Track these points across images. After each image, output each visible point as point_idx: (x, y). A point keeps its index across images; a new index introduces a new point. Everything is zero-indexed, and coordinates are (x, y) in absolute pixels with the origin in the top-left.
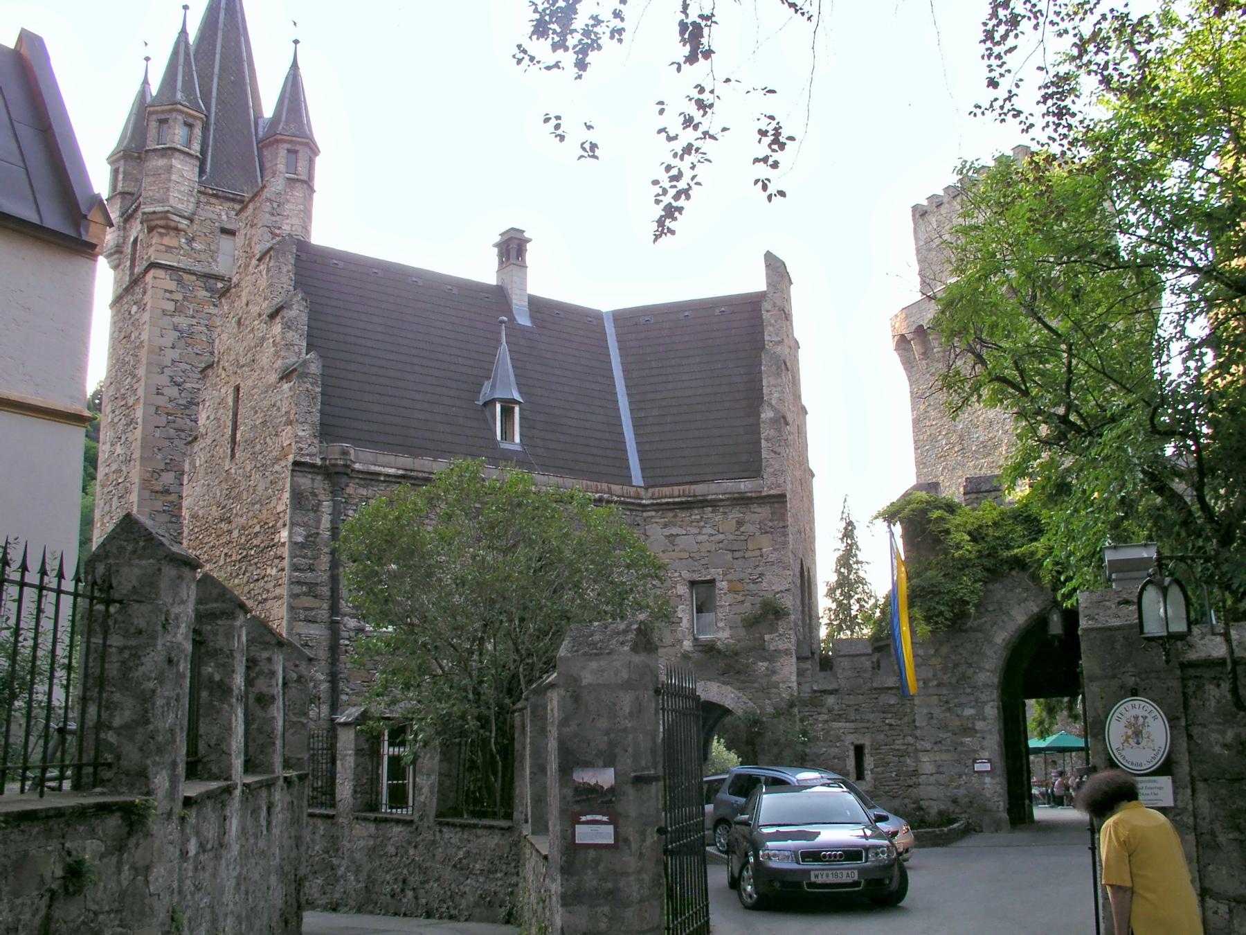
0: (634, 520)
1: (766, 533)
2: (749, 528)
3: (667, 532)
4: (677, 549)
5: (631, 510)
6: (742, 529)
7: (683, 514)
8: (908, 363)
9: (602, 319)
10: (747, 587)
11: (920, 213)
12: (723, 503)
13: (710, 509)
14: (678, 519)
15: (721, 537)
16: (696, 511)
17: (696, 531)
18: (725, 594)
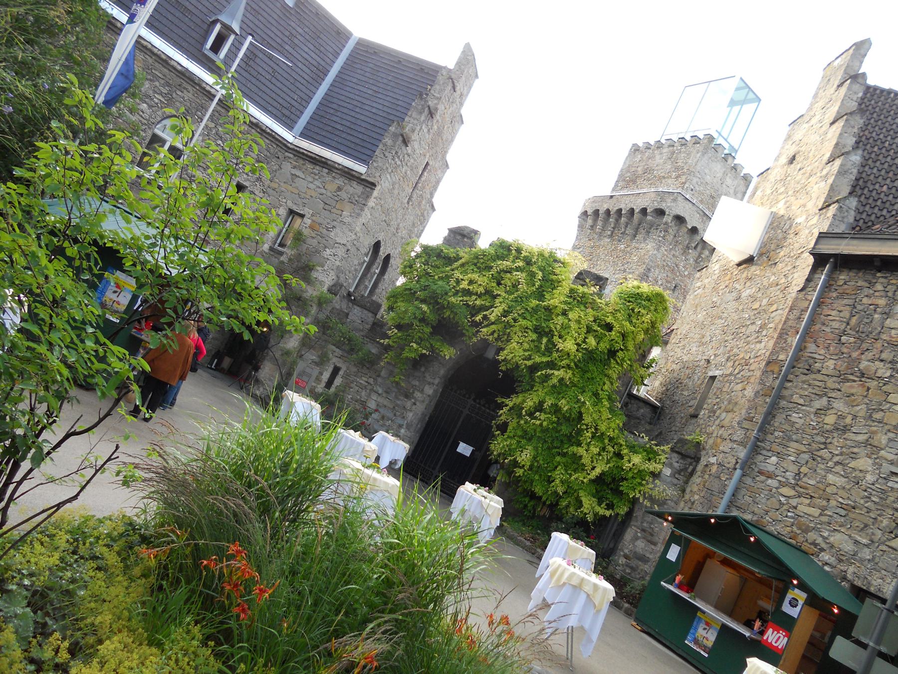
0: (277, 153)
1: (351, 203)
2: (343, 194)
3: (294, 171)
4: (294, 185)
5: (278, 145)
6: (338, 193)
7: (309, 166)
8: (581, 227)
9: (349, 38)
10: (321, 230)
11: (635, 149)
12: (336, 171)
13: (327, 171)
14: (305, 167)
15: (324, 191)
16: (318, 167)
17: (310, 179)
18: (306, 227)
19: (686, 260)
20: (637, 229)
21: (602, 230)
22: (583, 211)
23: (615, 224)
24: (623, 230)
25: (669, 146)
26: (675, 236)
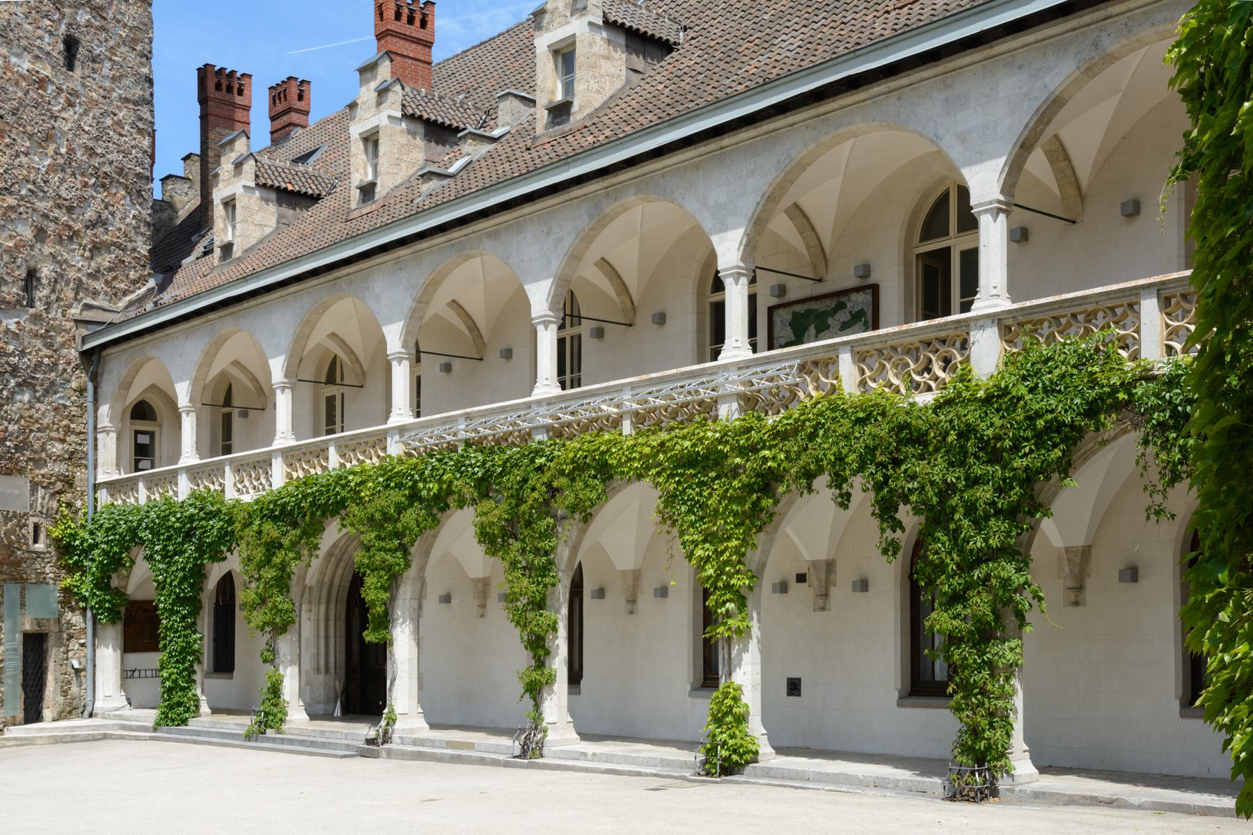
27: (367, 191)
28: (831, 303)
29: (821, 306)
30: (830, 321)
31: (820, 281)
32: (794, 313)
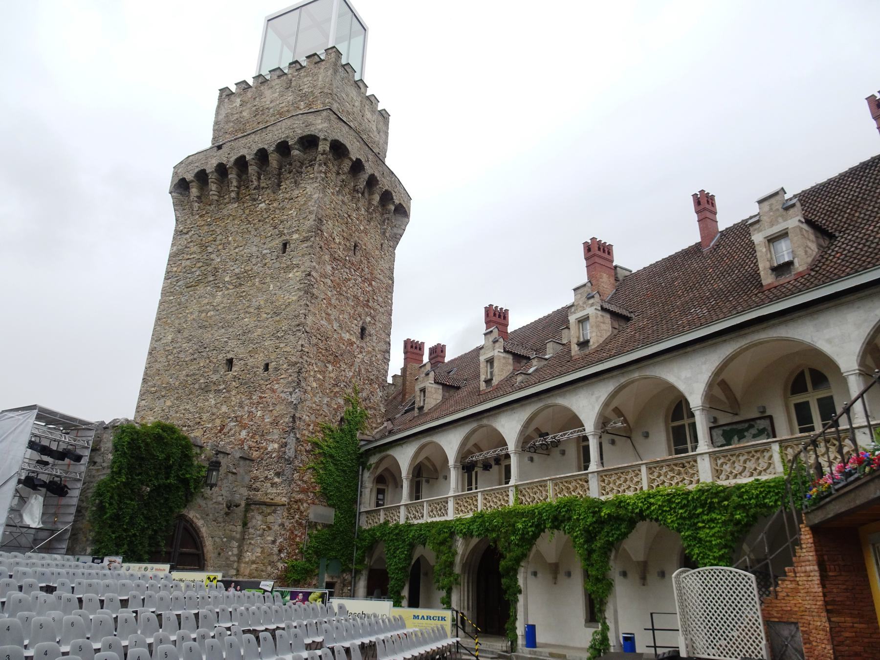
8: (178, 205)
11: (225, 94)
19: (358, 209)
20: (280, 174)
21: (220, 197)
22: (176, 181)
23: (239, 181)
24: (256, 183)
25: (279, 77)
26: (338, 174)
27: (488, 382)
28: (746, 425)
29: (740, 427)
30: (746, 434)
31: (736, 414)
32: (723, 430)
